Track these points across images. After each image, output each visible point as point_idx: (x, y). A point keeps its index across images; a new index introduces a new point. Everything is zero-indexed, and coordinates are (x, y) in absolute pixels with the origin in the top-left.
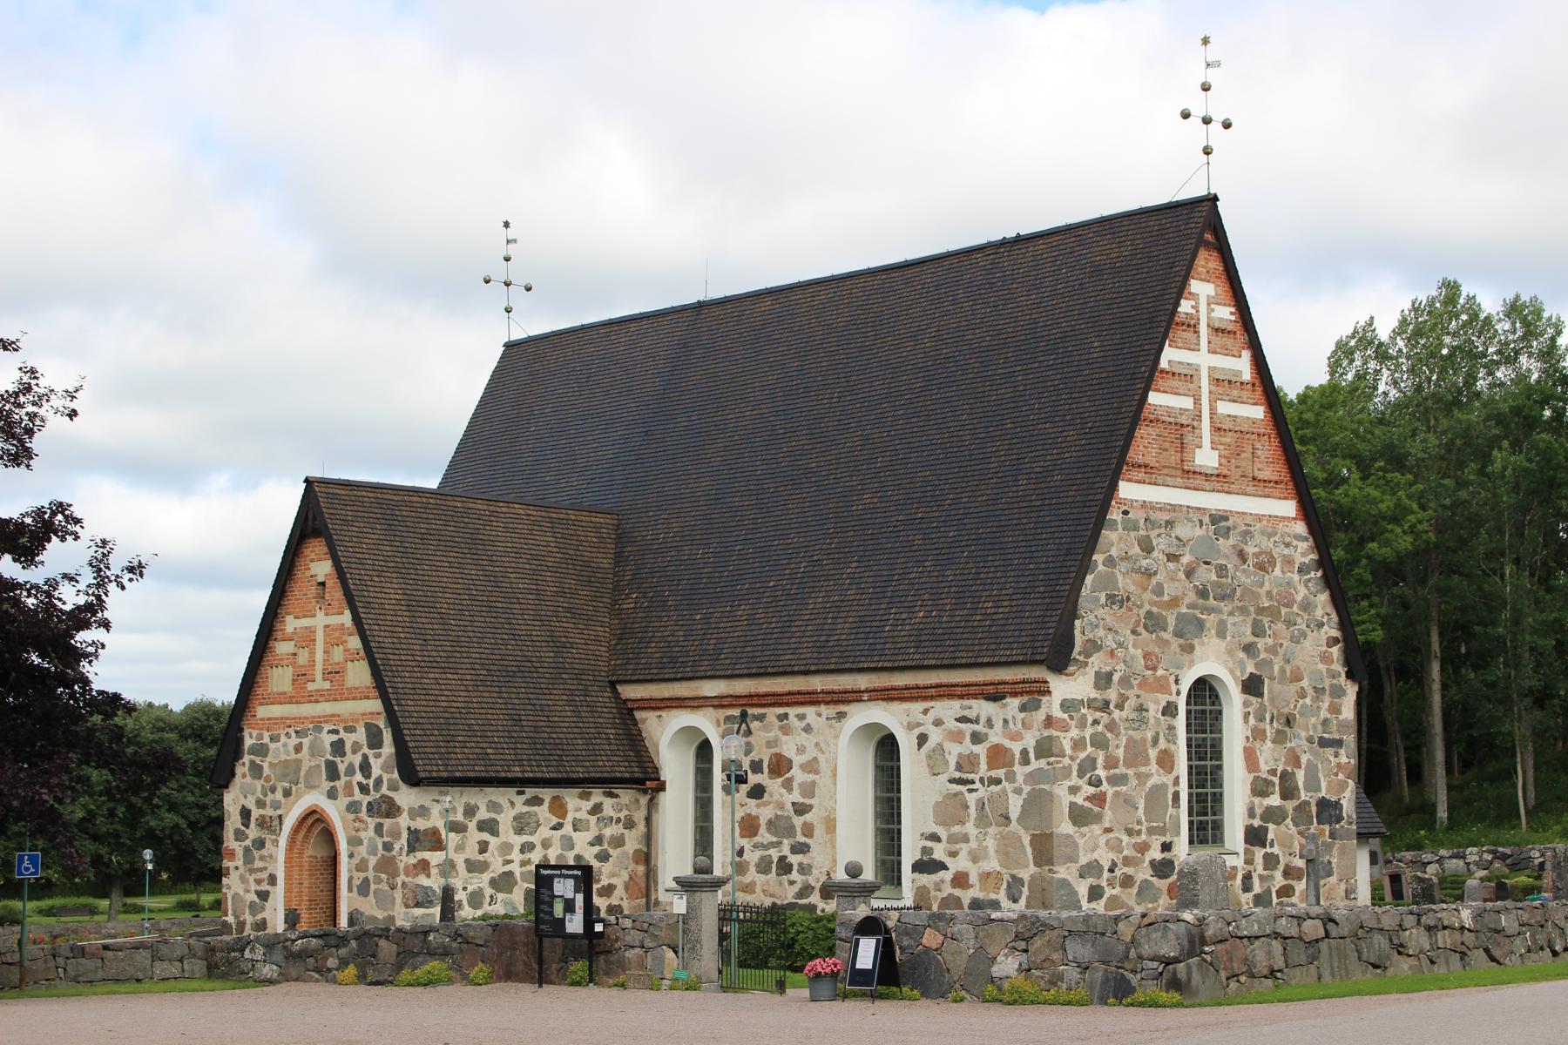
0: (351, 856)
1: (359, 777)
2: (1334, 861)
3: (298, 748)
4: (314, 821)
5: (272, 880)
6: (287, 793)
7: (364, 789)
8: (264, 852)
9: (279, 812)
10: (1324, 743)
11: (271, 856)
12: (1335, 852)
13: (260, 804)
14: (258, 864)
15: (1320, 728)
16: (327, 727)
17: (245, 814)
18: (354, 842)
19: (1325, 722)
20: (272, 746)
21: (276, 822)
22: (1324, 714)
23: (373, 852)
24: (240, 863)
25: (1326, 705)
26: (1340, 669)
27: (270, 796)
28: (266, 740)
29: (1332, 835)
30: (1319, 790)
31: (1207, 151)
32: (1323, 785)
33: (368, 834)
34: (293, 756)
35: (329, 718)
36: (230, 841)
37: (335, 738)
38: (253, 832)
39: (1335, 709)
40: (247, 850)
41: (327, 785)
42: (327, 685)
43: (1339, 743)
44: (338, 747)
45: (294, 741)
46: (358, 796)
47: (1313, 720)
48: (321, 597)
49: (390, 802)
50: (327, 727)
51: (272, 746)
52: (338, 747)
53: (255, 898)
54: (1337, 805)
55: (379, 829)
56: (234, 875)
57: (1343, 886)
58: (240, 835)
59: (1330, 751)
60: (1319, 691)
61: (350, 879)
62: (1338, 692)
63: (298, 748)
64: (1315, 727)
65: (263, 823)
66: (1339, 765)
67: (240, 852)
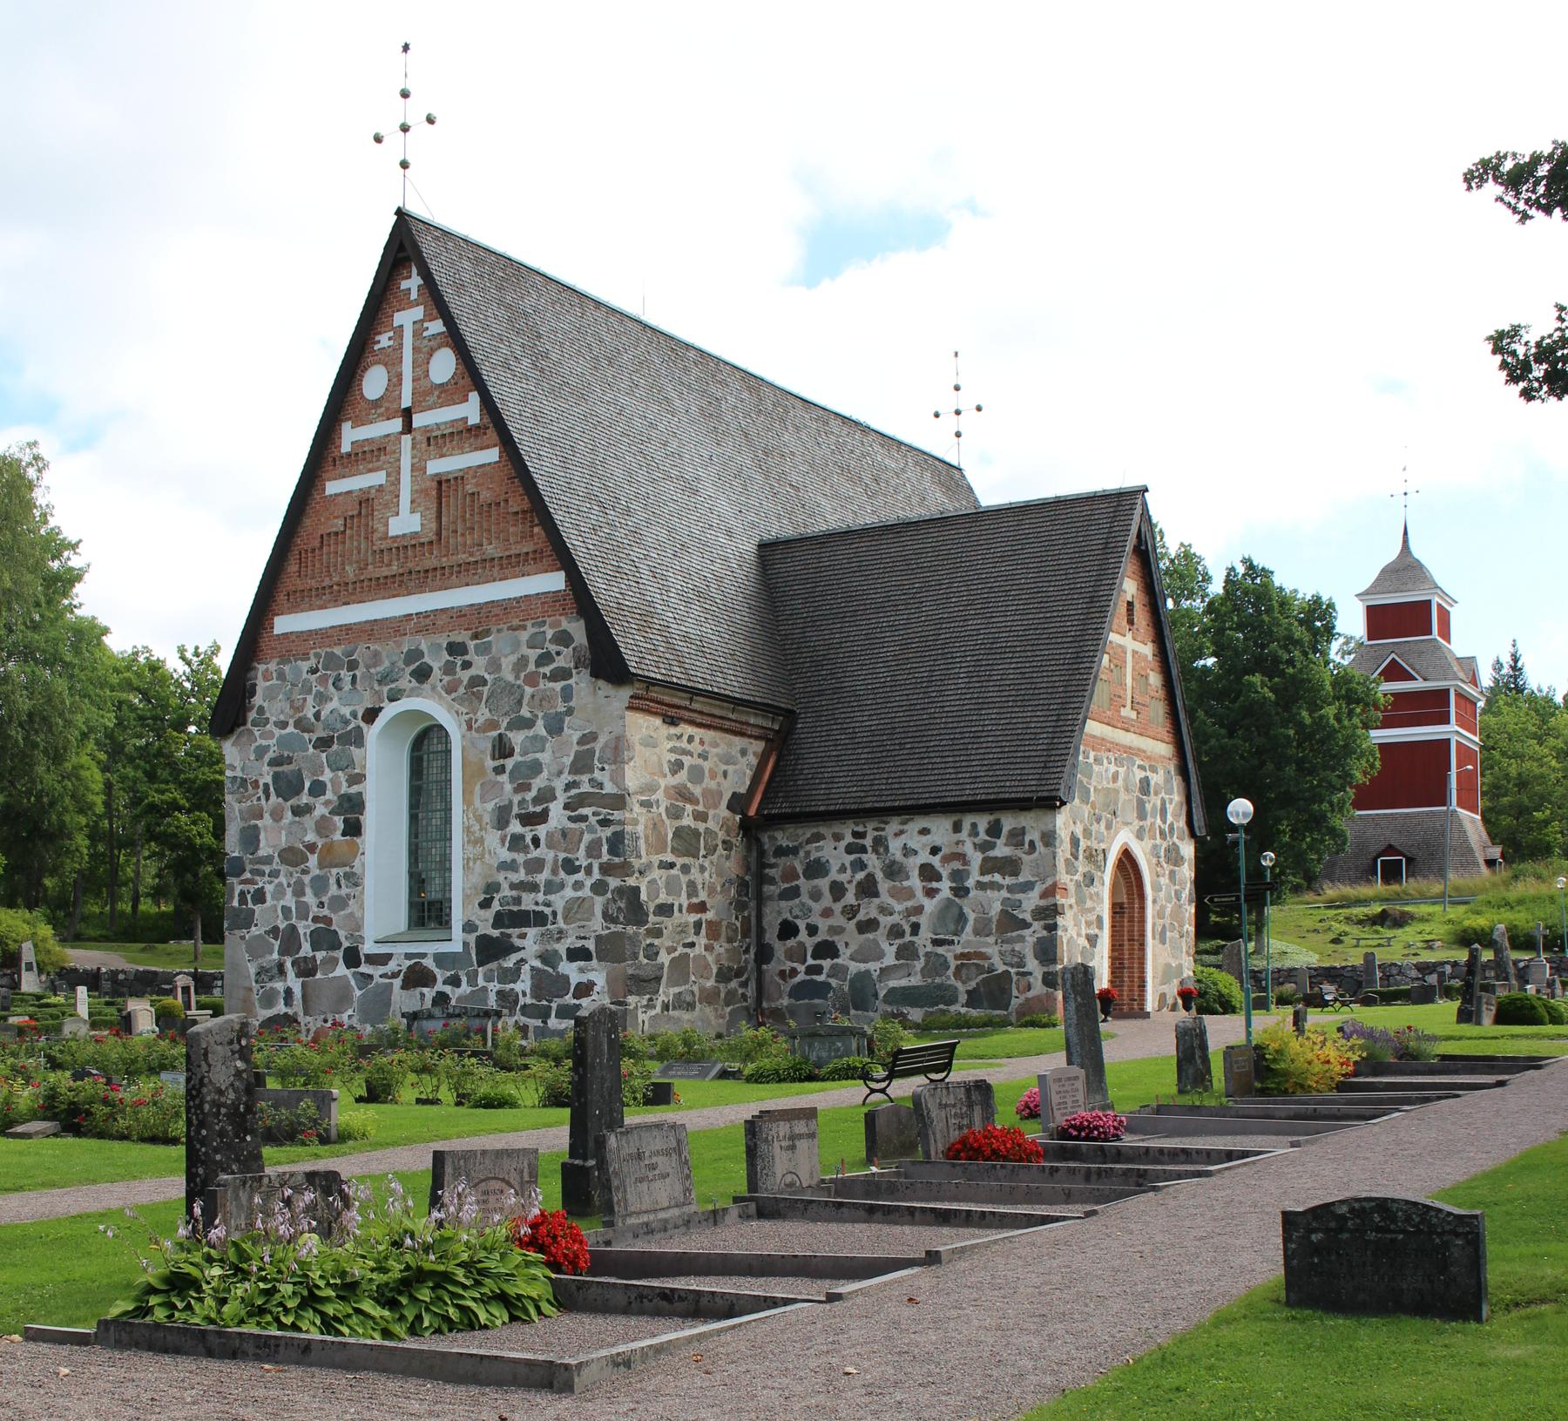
0: (1154, 901)
1: (1159, 821)
3: (1115, 777)
4: (1127, 862)
5: (1099, 919)
6: (1108, 827)
7: (1162, 833)
8: (1093, 890)
9: (1103, 846)
11: (1097, 894)
13: (1087, 833)
14: (1089, 904)
16: (1138, 762)
17: (1075, 842)
18: (1157, 888)
20: (1096, 768)
21: (1101, 857)
23: (1169, 900)
24: (1072, 901)
27: (1095, 827)
28: (1091, 760)
31: (958, 435)
33: (1164, 881)
34: (1111, 785)
35: (1139, 752)
36: (1063, 878)
37: (1143, 774)
38: (1082, 866)
40: (1078, 885)
41: (1137, 824)
42: (1133, 715)
44: (1145, 786)
45: (1113, 768)
46: (1158, 841)
48: (1131, 622)
49: (1176, 848)
50: (1138, 762)
51: (1096, 768)
52: (1145, 786)
53: (1086, 943)
55: (1172, 874)
56: (1069, 914)
58: (1071, 869)
61: (1154, 925)
63: (1115, 777)
65: (1091, 856)
67: (1071, 887)
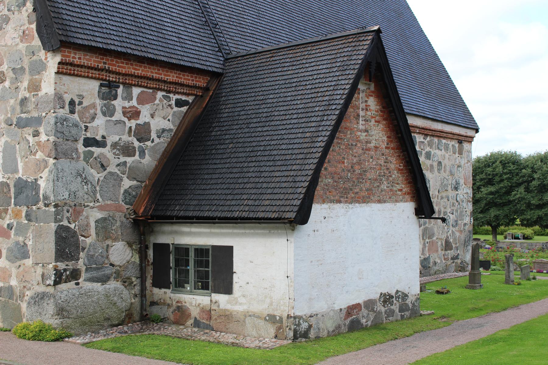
2: (30, 243)
10: (22, 124)
12: (30, 235)
15: (18, 108)
19: (24, 102)
22: (23, 93)
25: (26, 84)
26: (37, 42)
29: (28, 217)
30: (16, 171)
32: (20, 165)
39: (35, 87)
43: (39, 121)
47: (12, 101)
54: (35, 185)
57: (39, 270)
59: (29, 130)
60: (18, 72)
62: (38, 68)
64: (13, 109)
66: (39, 143)
